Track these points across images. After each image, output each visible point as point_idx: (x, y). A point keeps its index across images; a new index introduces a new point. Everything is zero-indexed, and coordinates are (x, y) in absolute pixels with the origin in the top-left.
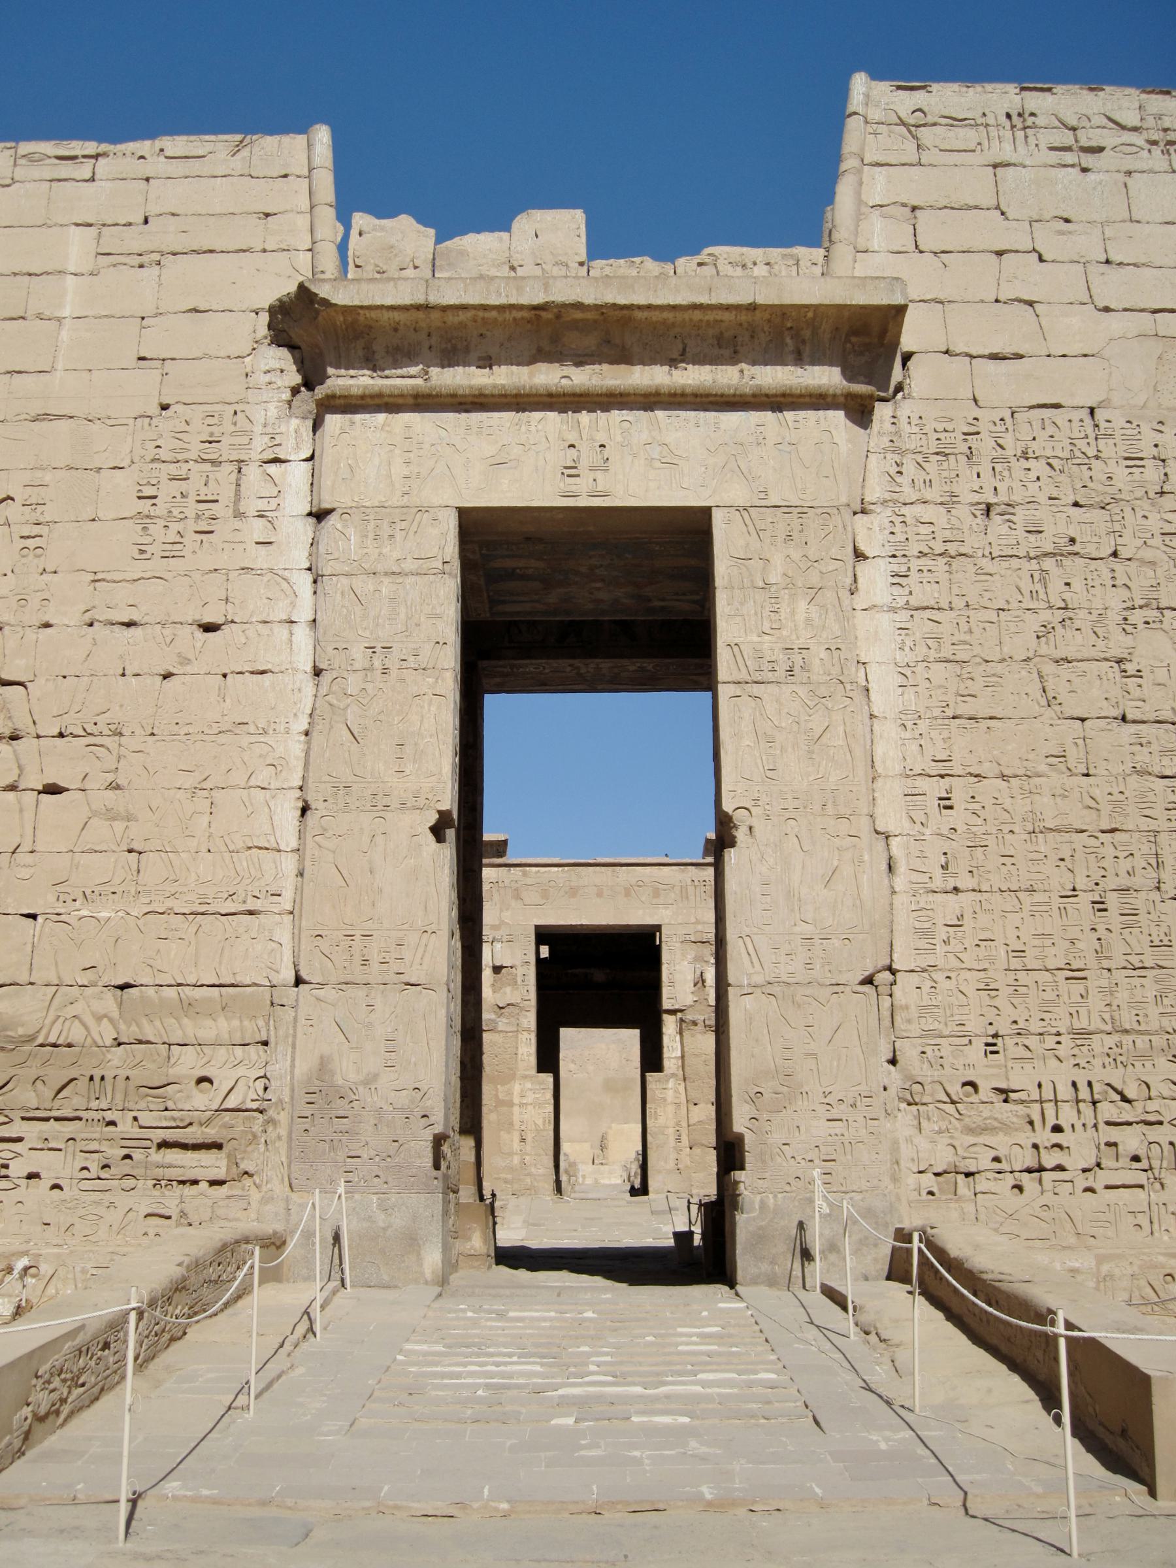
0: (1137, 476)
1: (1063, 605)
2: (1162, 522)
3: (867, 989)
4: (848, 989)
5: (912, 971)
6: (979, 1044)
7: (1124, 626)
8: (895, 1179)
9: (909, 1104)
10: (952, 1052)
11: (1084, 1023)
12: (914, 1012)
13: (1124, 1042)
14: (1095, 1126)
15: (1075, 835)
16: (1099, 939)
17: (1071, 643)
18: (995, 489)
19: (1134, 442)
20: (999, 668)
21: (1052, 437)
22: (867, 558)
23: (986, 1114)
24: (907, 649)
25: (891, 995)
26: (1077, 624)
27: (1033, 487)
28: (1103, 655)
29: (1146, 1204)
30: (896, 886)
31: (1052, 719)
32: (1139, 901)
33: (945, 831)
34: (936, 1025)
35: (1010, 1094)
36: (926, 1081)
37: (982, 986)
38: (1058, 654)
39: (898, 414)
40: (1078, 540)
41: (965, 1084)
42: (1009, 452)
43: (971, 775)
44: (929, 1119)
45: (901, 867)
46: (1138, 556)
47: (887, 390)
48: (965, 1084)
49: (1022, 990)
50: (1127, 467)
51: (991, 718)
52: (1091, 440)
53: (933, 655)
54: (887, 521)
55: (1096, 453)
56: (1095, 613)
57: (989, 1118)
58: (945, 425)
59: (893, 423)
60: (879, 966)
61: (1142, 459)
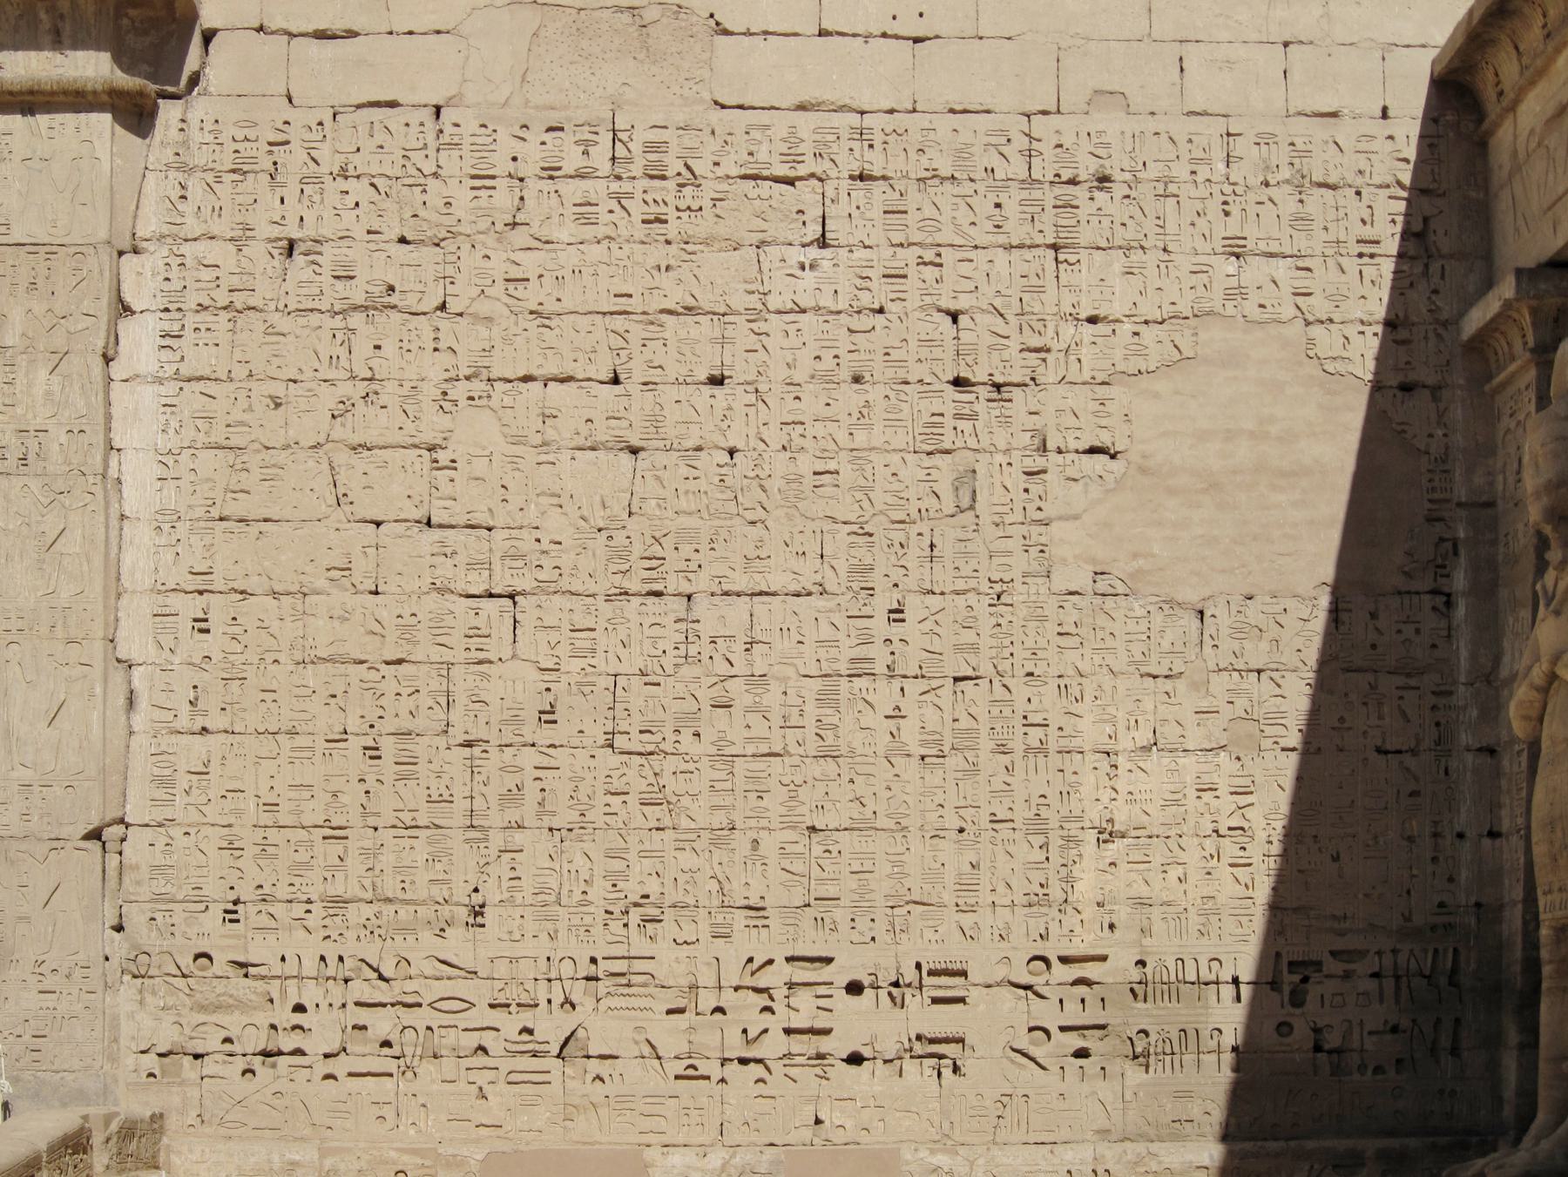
0: (483, 202)
1: (369, 375)
2: (508, 264)
3: (94, 846)
4: (69, 845)
5: (147, 825)
6: (217, 911)
7: (442, 403)
8: (113, 1059)
9: (135, 977)
10: (186, 919)
11: (337, 889)
12: (144, 873)
13: (385, 913)
14: (344, 1005)
15: (352, 668)
16: (367, 792)
17: (373, 424)
18: (302, 219)
19: (486, 154)
20: (282, 457)
21: (382, 147)
22: (133, 313)
23: (218, 991)
24: (171, 431)
25: (120, 854)
26: (383, 400)
27: (349, 217)
28: (411, 441)
29: (392, 1094)
30: (134, 725)
31: (340, 521)
32: (420, 747)
33: (197, 660)
34: (169, 889)
35: (252, 970)
36: (154, 951)
37: (225, 844)
38: (356, 439)
39: (189, 116)
40: (398, 289)
41: (198, 956)
42: (324, 169)
43: (236, 591)
44: (154, 993)
45: (143, 703)
46: (471, 310)
47: (176, 83)
48: (198, 956)
49: (271, 850)
50: (473, 188)
51: (266, 520)
52: (431, 152)
53: (202, 439)
54: (161, 263)
55: (434, 170)
56: (407, 385)
57: (224, 994)
58: (246, 131)
59: (182, 130)
60: (108, 819)
61: (493, 177)
